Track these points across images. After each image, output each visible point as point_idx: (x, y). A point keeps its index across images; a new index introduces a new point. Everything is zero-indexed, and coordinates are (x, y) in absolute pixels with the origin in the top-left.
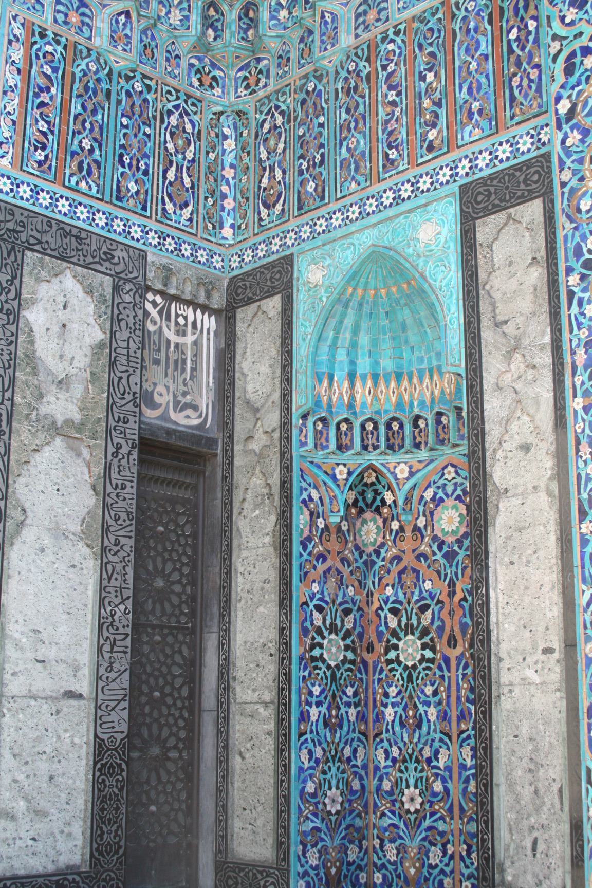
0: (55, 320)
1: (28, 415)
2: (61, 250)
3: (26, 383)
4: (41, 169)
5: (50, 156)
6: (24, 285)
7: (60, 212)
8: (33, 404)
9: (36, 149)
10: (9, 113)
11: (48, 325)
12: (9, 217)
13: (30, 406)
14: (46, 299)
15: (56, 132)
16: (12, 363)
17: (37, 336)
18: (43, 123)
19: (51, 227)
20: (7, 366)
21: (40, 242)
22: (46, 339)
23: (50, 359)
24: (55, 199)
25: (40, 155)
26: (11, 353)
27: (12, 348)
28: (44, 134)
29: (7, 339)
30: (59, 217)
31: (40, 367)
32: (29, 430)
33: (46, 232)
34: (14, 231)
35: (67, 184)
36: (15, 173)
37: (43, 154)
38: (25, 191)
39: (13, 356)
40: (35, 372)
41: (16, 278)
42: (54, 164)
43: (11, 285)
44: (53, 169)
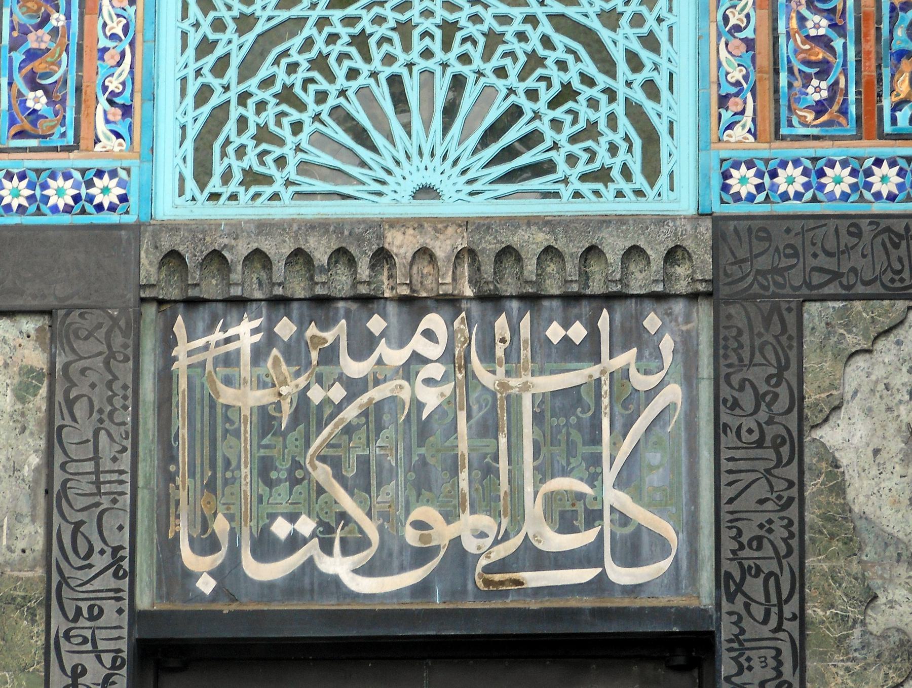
0: (892, 427)
1: (840, 640)
2: (886, 279)
3: (833, 574)
4: (825, 118)
5: (842, 84)
6: (808, 377)
7: (878, 196)
8: (853, 613)
9: (807, 79)
10: (738, 28)
11: (876, 443)
12: (758, 247)
13: (845, 619)
14: (865, 389)
15: (851, 26)
16: (794, 543)
17: (851, 475)
18: (817, 18)
19: (859, 235)
20: (783, 550)
21: (836, 276)
22: (874, 471)
23: (887, 511)
24: (861, 172)
25: (818, 90)
26: (791, 523)
27: (793, 512)
28: (824, 42)
29: (779, 498)
30: (879, 208)
31: (865, 535)
32: (848, 669)
33: (848, 250)
34: (776, 271)
35: (888, 128)
36: (763, 150)
37: (824, 85)
38: (791, 180)
39: (795, 528)
40: (852, 546)
41: (787, 367)
42: (852, 96)
43: (777, 385)
44: (852, 109)
